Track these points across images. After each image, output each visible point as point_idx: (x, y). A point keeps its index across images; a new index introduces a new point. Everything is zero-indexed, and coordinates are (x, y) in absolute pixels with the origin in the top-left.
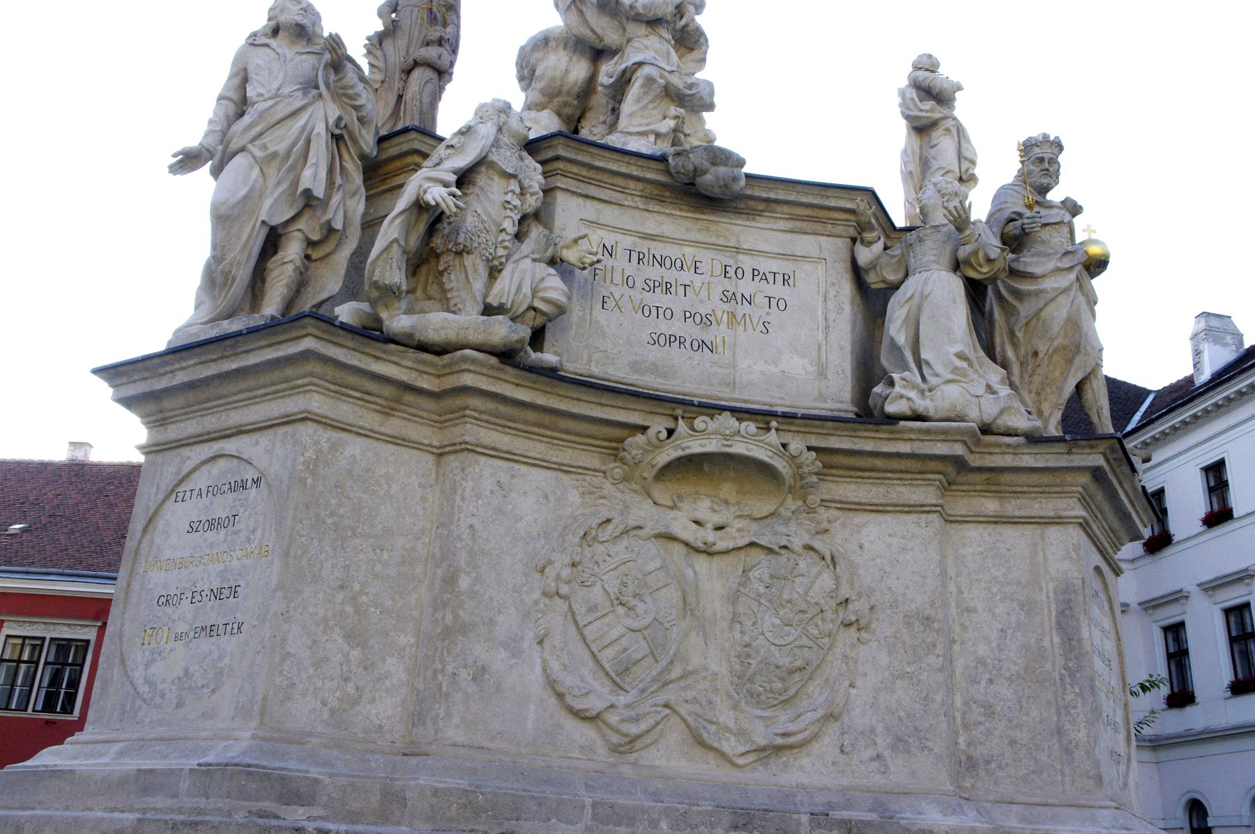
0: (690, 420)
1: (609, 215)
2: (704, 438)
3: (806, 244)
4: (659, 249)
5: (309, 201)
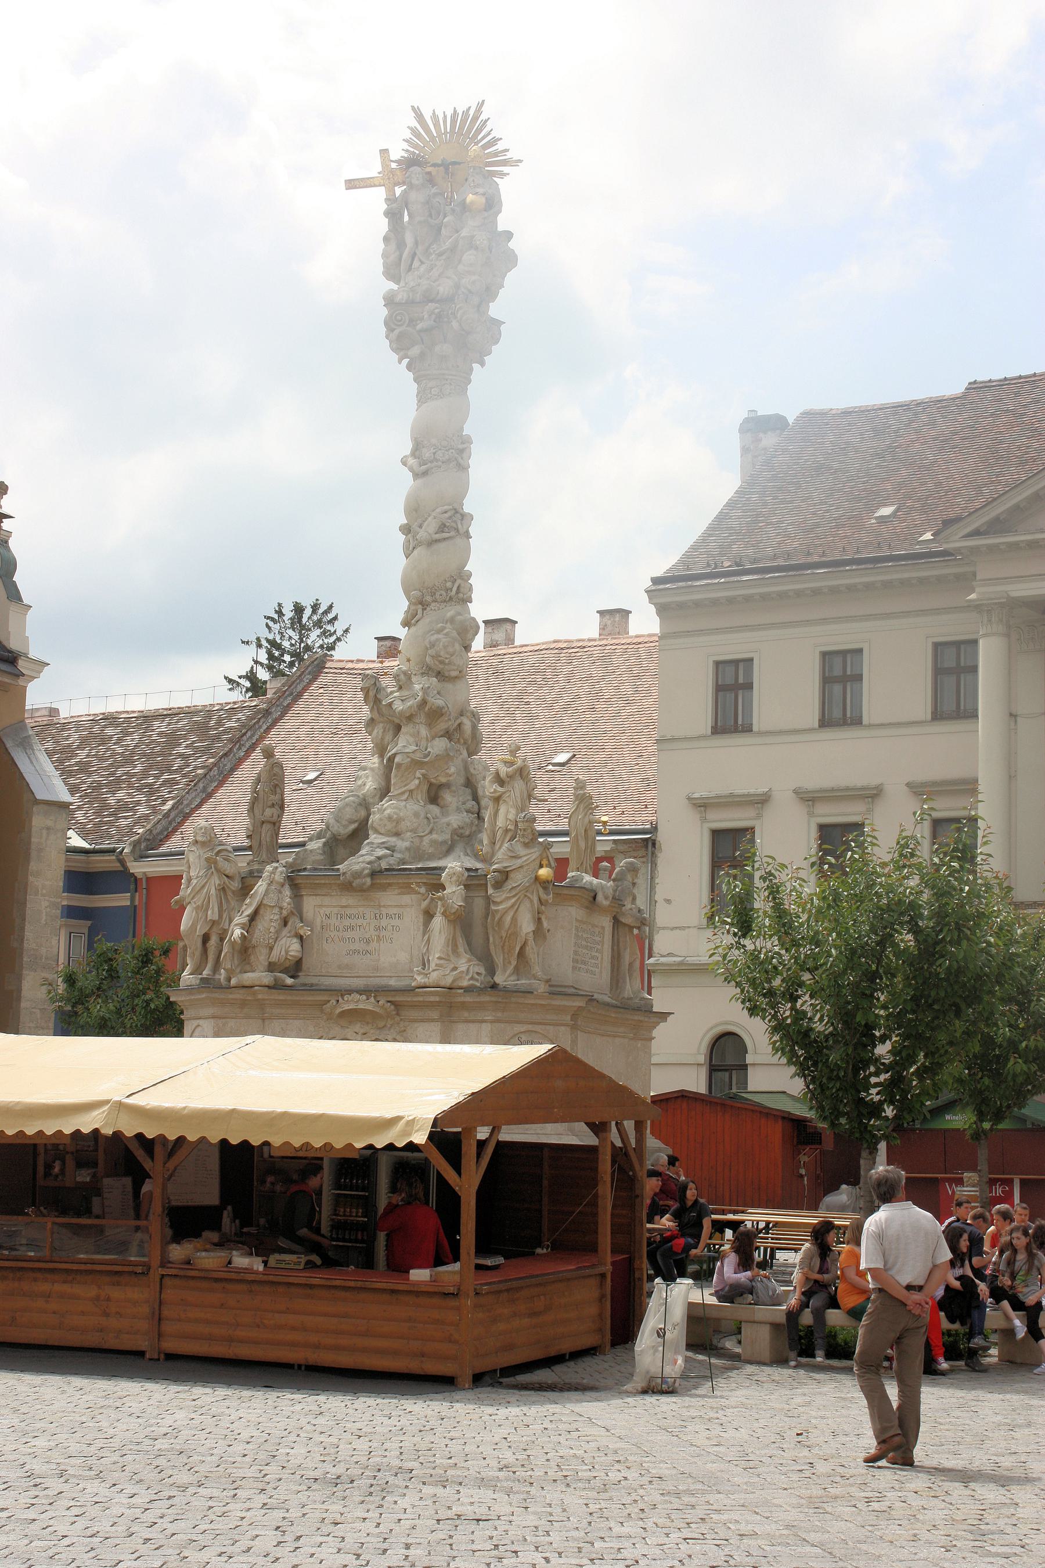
0: (342, 996)
1: (327, 900)
2: (349, 1003)
3: (407, 899)
4: (349, 911)
5: (214, 923)
